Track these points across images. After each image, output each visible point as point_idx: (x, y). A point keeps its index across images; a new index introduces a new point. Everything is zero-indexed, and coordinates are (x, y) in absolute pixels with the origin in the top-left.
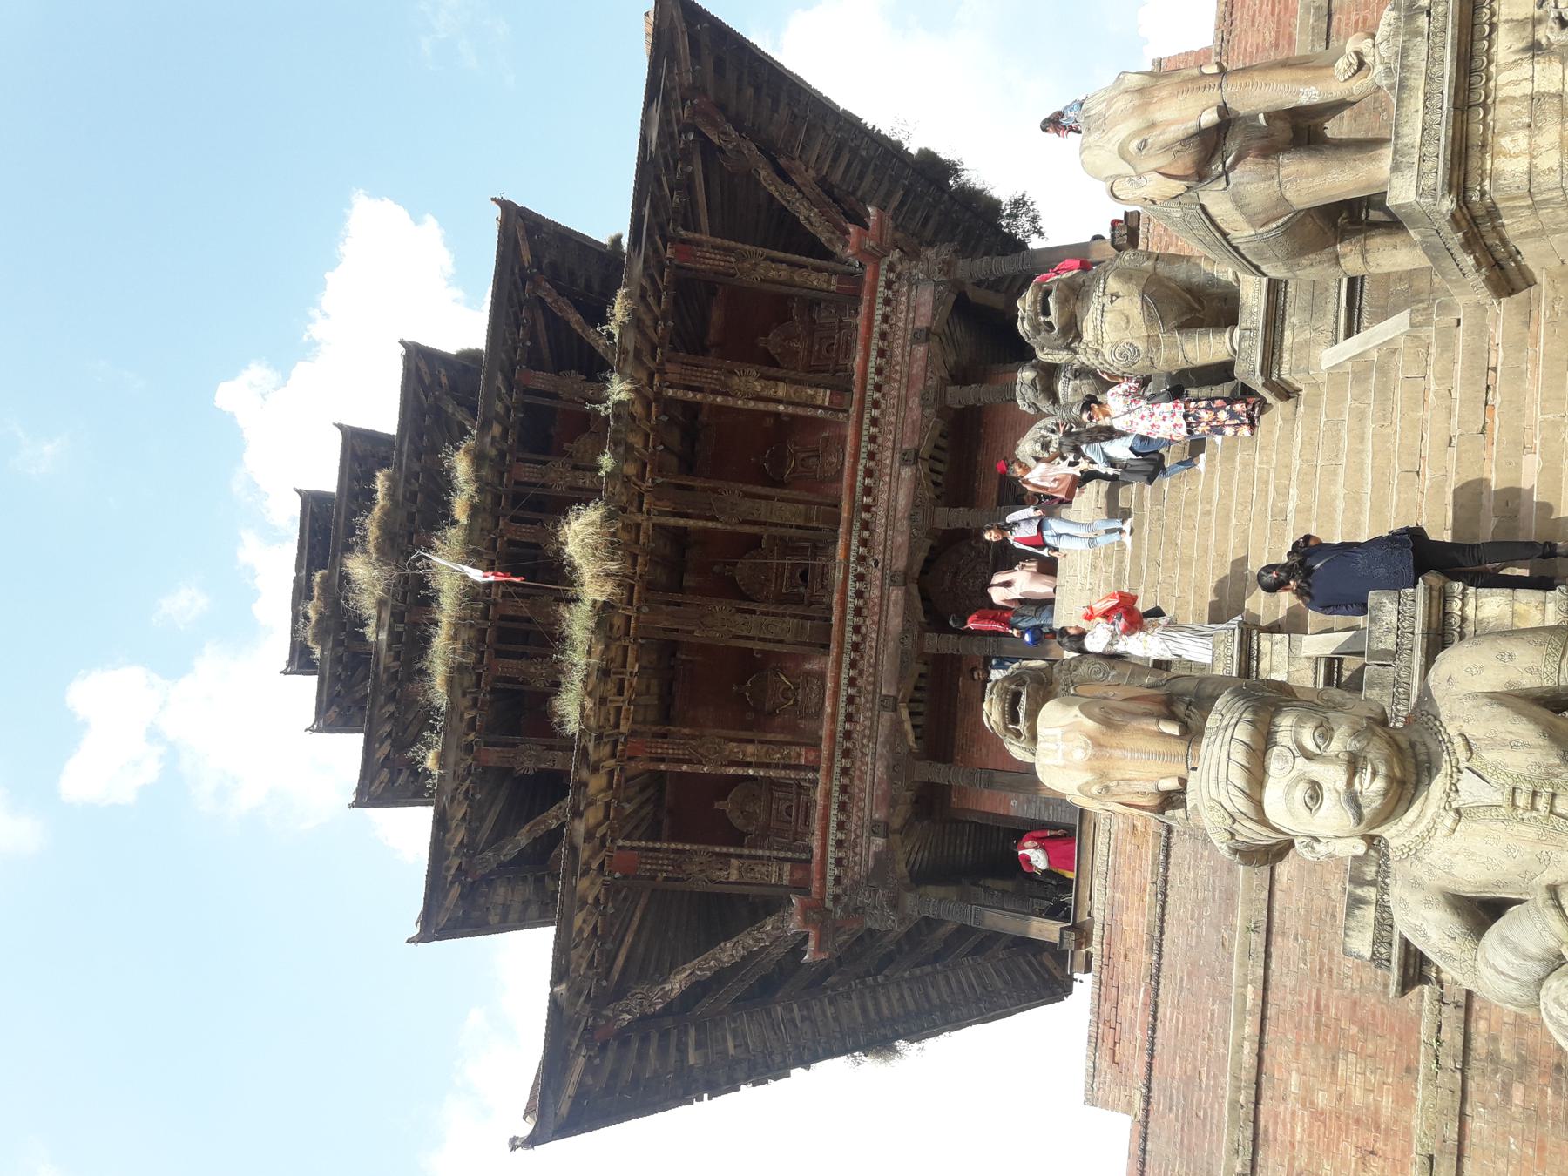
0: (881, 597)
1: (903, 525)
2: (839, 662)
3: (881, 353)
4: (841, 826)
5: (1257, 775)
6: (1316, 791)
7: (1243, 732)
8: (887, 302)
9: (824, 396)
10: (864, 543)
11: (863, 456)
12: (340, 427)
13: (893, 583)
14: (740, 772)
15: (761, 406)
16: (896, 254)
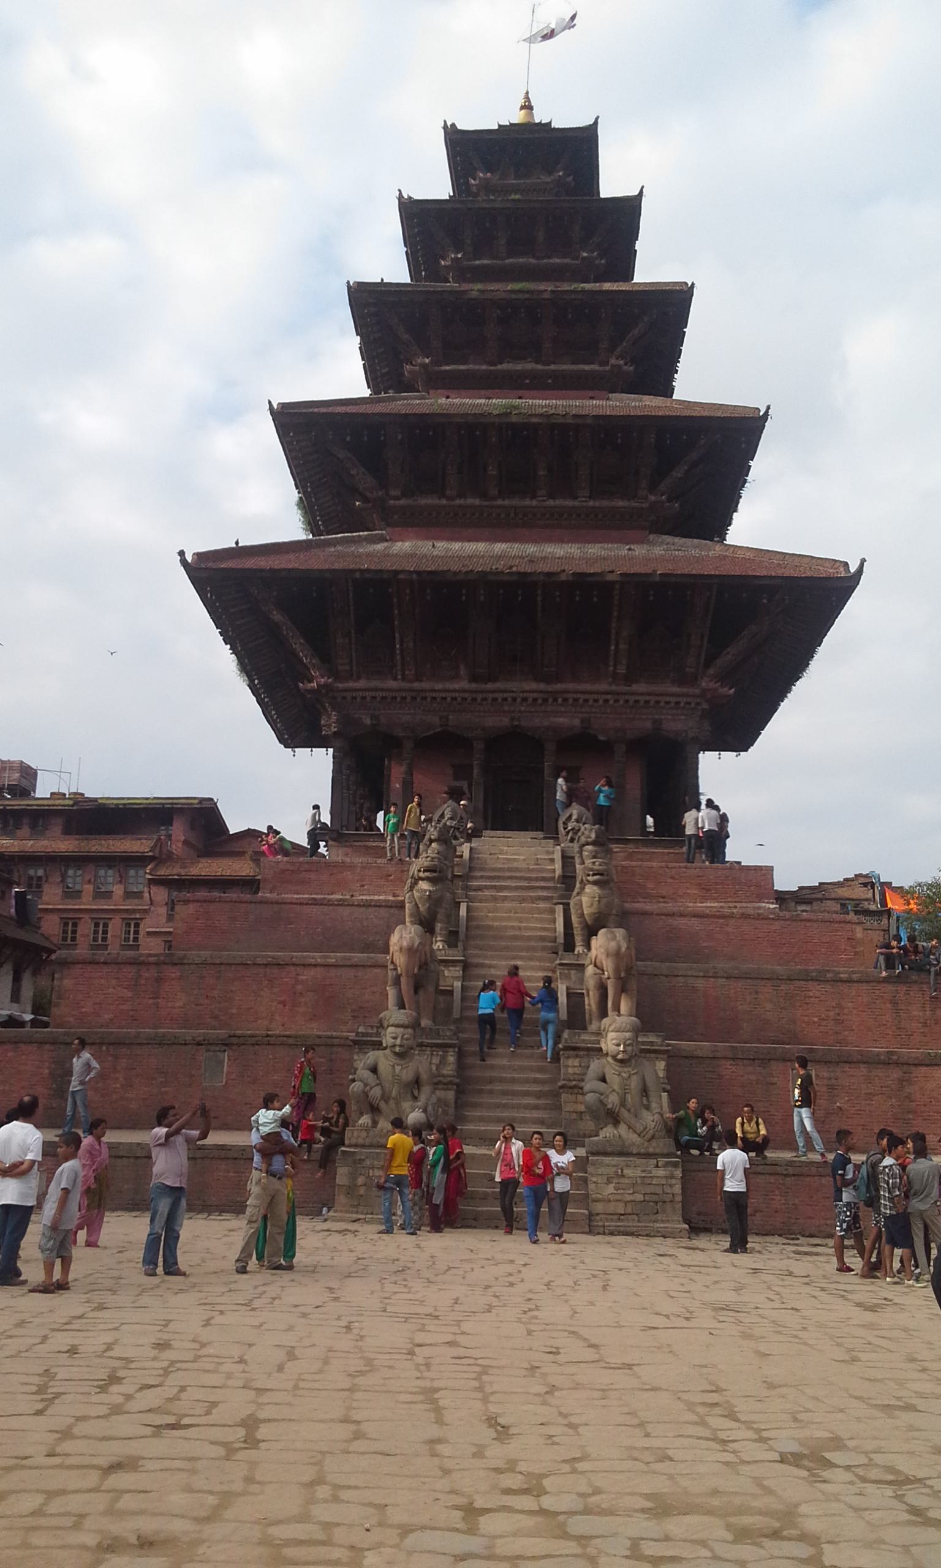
0: (504, 712)
1: (546, 723)
2: (464, 691)
3: (647, 702)
4: (374, 698)
5: (397, 1026)
6: (395, 1038)
7: (406, 1023)
8: (677, 703)
9: (622, 670)
10: (535, 700)
11: (586, 696)
12: (641, 192)
13: (512, 719)
14: (397, 641)
15: (613, 637)
16: (705, 706)
